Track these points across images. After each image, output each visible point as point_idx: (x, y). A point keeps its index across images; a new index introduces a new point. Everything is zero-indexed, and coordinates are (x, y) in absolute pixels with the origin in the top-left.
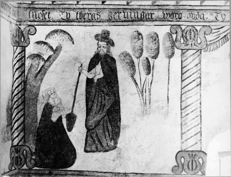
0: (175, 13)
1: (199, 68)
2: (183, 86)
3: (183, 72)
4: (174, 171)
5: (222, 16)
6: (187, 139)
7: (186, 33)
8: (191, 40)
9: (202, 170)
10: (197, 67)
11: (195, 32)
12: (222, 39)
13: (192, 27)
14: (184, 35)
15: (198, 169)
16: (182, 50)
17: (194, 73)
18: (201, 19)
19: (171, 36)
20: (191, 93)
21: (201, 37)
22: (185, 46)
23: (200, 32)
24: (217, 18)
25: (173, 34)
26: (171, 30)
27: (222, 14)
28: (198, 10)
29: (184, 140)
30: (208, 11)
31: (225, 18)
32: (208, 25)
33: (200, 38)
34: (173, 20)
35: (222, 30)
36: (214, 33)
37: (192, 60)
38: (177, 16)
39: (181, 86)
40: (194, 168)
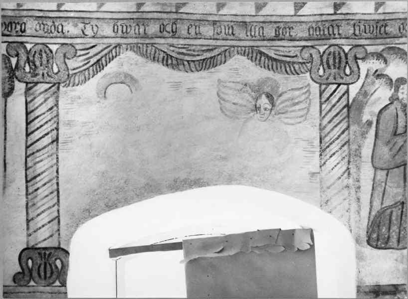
0: (14, 22)
1: (55, 113)
2: (29, 143)
3: (29, 121)
4: (17, 281)
5: (92, 28)
6: (37, 229)
7: (34, 56)
8: (42, 68)
9: (61, 277)
10: (51, 111)
11: (48, 55)
12: (93, 65)
13: (43, 46)
14: (31, 58)
15: (54, 276)
16: (27, 83)
17: (47, 122)
18: (59, 32)
19: (9, 60)
20: (41, 154)
21: (58, 63)
22: (32, 77)
23: (57, 55)
24: (85, 31)
25: (13, 57)
26: (8, 50)
27: (92, 26)
28: (53, 18)
29: (31, 231)
30: (70, 20)
31: (97, 31)
32: (71, 42)
33: (57, 65)
34: (11, 34)
35: (92, 52)
36: (80, 56)
37: (43, 100)
38: (18, 27)
39: (26, 144)
40: (48, 275)
